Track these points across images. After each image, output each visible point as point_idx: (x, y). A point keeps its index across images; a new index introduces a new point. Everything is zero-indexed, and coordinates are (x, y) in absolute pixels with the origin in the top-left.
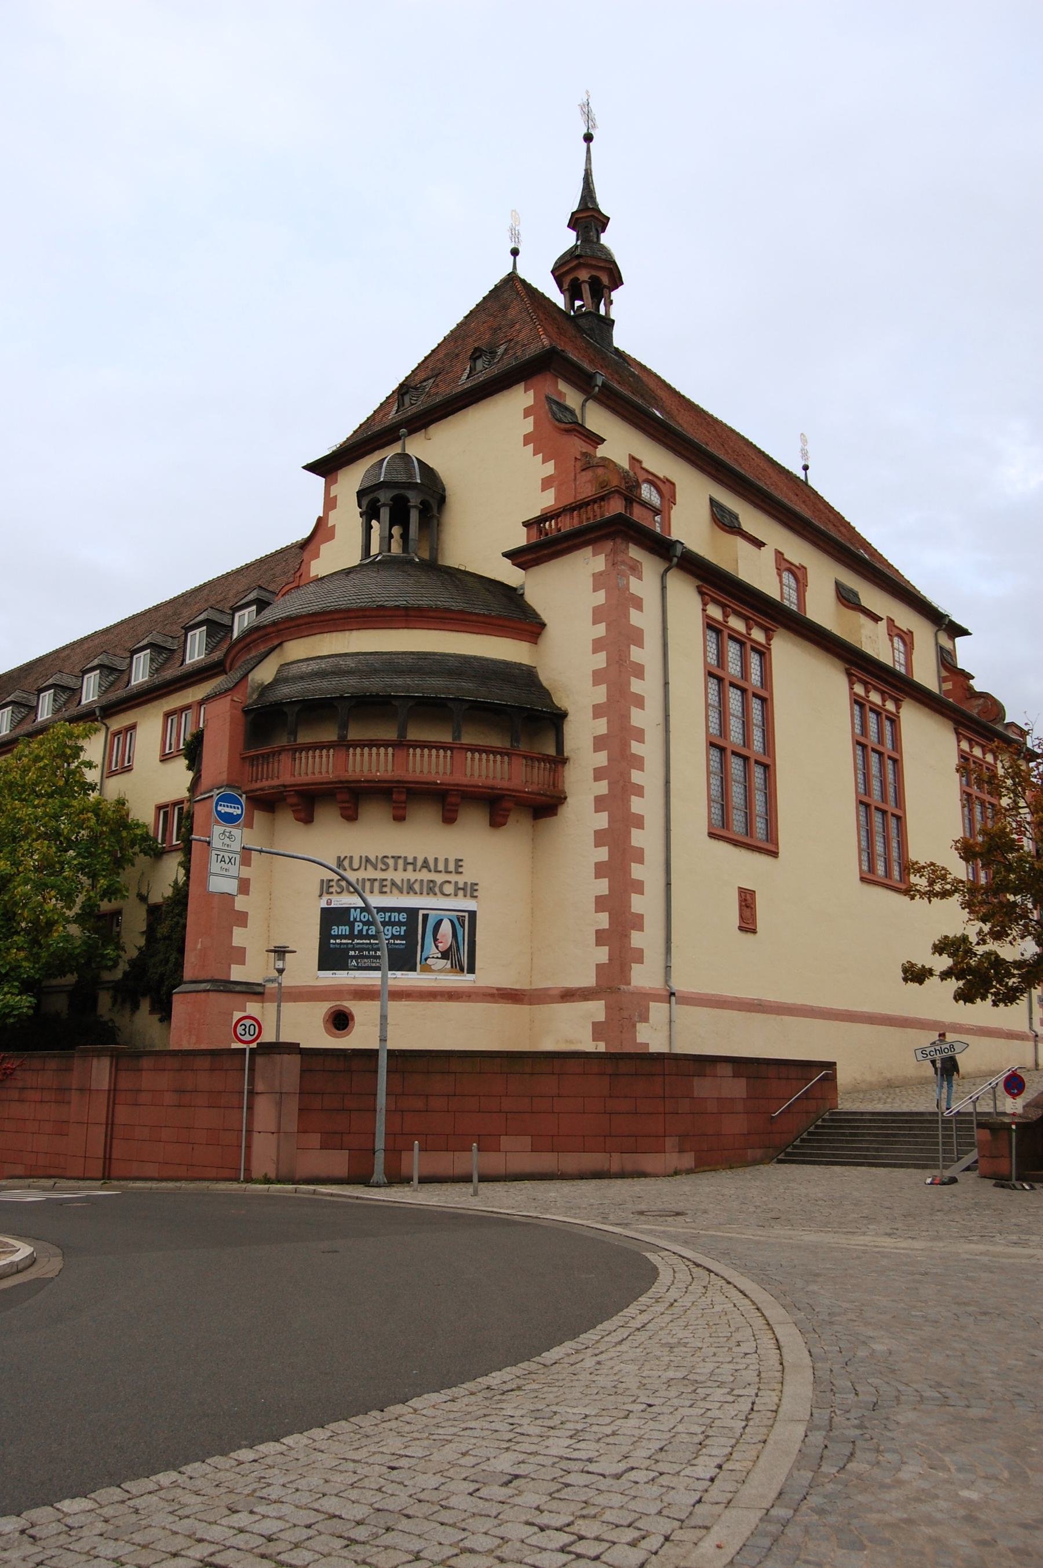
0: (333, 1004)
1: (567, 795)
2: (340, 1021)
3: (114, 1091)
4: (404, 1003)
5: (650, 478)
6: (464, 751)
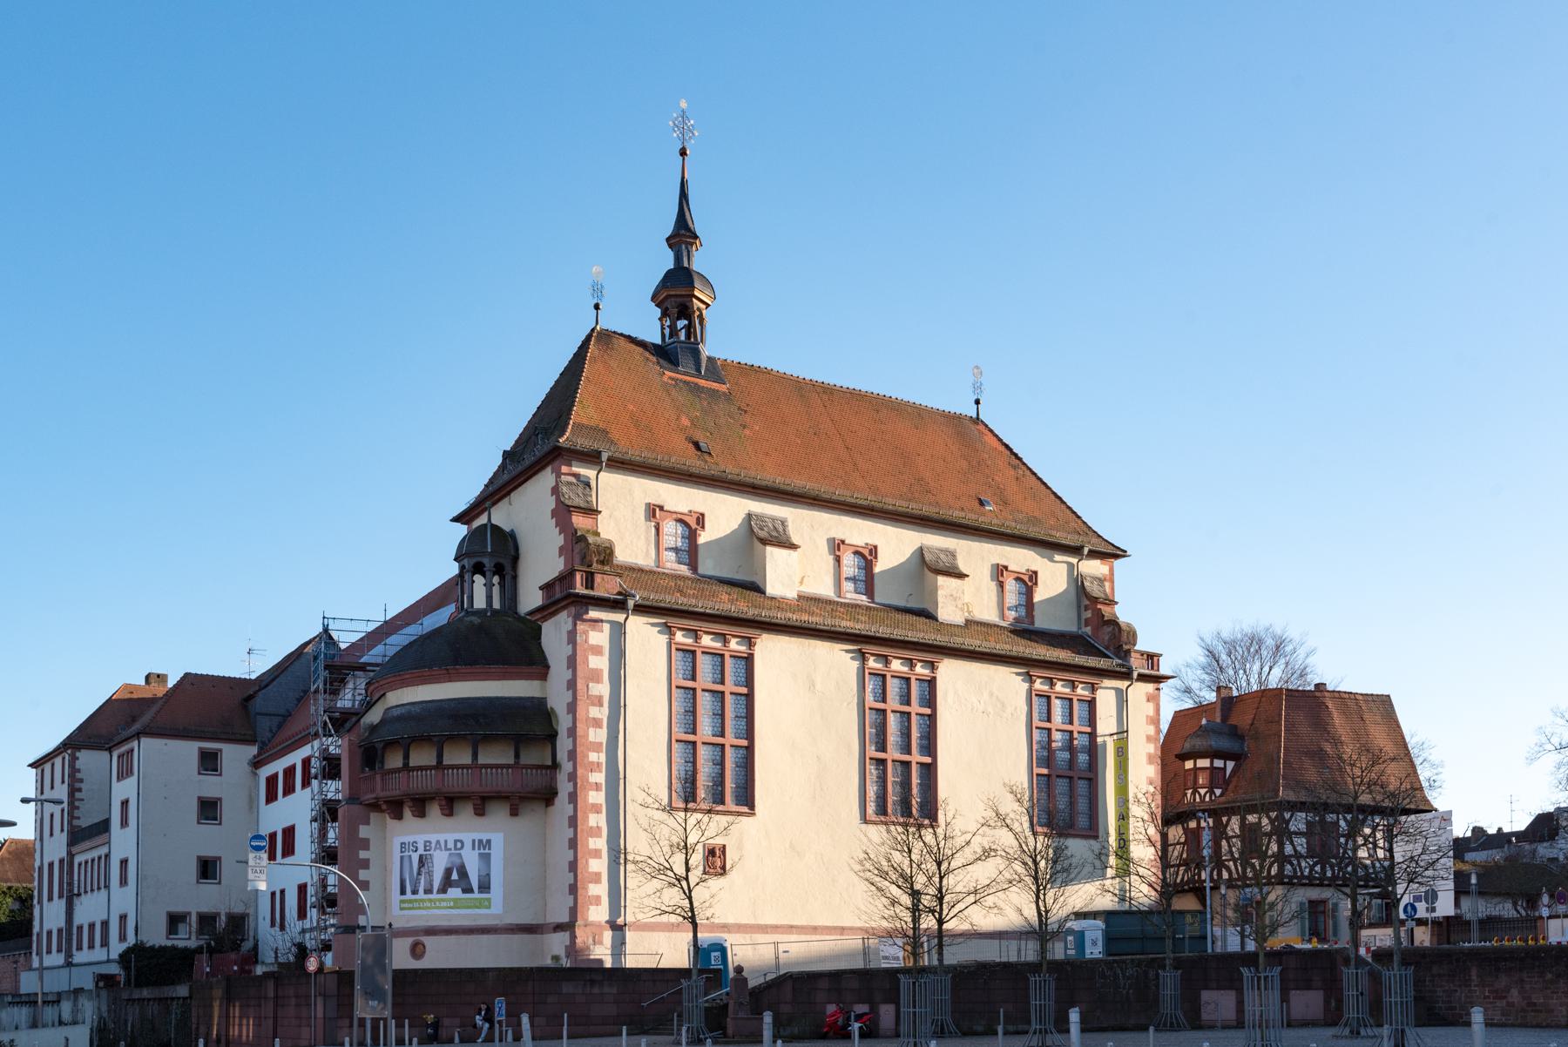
1: (559, 791)
2: (417, 951)
3: (276, 997)
6: (478, 769)
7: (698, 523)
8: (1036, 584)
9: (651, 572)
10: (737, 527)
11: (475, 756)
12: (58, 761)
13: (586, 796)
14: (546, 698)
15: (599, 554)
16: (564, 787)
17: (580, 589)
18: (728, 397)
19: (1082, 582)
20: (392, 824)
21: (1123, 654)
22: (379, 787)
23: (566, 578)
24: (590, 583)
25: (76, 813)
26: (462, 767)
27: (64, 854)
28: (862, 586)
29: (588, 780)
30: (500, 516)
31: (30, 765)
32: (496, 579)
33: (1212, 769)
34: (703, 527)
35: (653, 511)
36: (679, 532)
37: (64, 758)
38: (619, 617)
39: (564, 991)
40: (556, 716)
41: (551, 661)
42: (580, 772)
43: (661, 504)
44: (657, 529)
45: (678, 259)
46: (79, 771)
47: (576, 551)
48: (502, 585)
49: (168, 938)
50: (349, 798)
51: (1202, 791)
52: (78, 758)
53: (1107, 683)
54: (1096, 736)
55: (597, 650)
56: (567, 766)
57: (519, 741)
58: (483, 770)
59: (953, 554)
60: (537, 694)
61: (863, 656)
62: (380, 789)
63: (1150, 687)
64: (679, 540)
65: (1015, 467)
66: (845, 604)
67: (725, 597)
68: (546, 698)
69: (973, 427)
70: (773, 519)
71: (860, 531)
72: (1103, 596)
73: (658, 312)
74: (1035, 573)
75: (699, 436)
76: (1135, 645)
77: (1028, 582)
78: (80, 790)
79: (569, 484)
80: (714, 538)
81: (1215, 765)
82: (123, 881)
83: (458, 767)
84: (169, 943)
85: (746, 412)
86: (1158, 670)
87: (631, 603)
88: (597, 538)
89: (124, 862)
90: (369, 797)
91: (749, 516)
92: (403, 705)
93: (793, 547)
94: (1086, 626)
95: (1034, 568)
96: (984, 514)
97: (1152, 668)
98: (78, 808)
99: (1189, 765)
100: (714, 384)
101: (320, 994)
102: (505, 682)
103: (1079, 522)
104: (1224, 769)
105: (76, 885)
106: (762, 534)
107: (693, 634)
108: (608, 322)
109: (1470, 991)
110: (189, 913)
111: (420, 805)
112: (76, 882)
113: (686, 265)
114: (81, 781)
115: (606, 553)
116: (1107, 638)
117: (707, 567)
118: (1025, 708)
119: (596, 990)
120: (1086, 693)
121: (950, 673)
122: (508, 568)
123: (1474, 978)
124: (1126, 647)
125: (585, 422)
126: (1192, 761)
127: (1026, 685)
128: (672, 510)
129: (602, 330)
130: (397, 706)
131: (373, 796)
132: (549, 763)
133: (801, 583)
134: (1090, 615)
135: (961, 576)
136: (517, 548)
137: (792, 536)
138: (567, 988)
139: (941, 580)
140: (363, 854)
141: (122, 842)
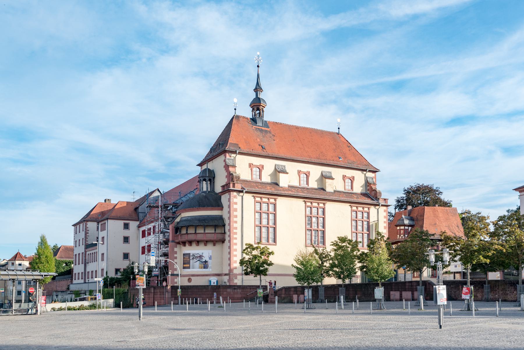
0: (189, 277)
2: (190, 280)
3: (154, 292)
4: (199, 277)
5: (256, 166)
9: (250, 181)
11: (205, 230)
12: (81, 225)
13: (233, 241)
14: (222, 215)
16: (227, 239)
17: (231, 188)
20: (183, 247)
21: (377, 199)
22: (180, 239)
23: (227, 185)
24: (234, 186)
25: (87, 240)
26: (201, 233)
27: (84, 251)
29: (233, 237)
30: (210, 166)
31: (73, 225)
32: (209, 182)
33: (405, 229)
37: (83, 224)
39: (228, 291)
40: (225, 220)
41: (224, 206)
42: (231, 235)
45: (257, 95)
46: (88, 228)
47: (230, 177)
48: (210, 184)
49: (115, 276)
50: (172, 241)
51: (402, 235)
52: (87, 224)
56: (228, 233)
57: (216, 227)
58: (207, 234)
59: (331, 173)
60: (220, 214)
61: (305, 202)
62: (180, 239)
63: (385, 208)
65: (349, 147)
67: (269, 188)
68: (222, 215)
69: (337, 136)
72: (373, 183)
73: (251, 109)
75: (262, 144)
76: (381, 196)
78: (88, 233)
81: (405, 228)
82: (103, 260)
83: (200, 233)
84: (116, 277)
86: (387, 203)
87: (244, 191)
88: (236, 174)
89: (103, 254)
90: (177, 241)
92: (186, 217)
93: (287, 173)
94: (368, 191)
96: (339, 161)
97: (386, 203)
98: (87, 238)
99: (398, 228)
101: (167, 292)
103: (367, 162)
104: (408, 229)
105: (87, 260)
106: (279, 170)
108: (237, 114)
109: (460, 292)
110: (121, 269)
111: (190, 243)
112: (87, 259)
113: (259, 97)
114: (88, 230)
115: (238, 178)
116: (373, 194)
119: (236, 291)
121: (329, 206)
122: (212, 180)
123: (460, 288)
124: (378, 197)
125: (232, 142)
126: (399, 227)
129: (237, 115)
130: (184, 217)
131: (178, 240)
132: (223, 232)
134: (369, 188)
135: (333, 179)
136: (214, 175)
137: (287, 170)
138: (229, 290)
139: (327, 180)
140: (175, 255)
141: (101, 249)
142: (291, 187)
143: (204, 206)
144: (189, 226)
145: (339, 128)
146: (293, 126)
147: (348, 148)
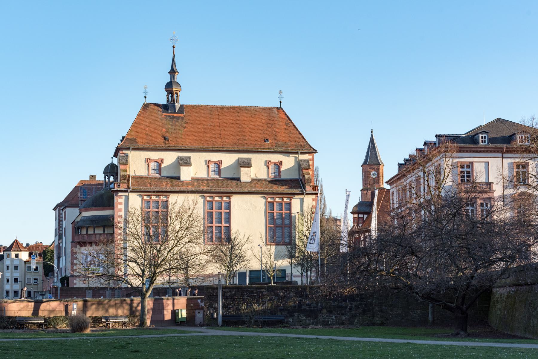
7: (161, 162)
8: (282, 165)
10: (174, 161)
15: (123, 178)
18: (183, 118)
19: (300, 163)
22: (80, 238)
24: (119, 186)
28: (217, 173)
31: (53, 210)
34: (163, 163)
35: (147, 160)
36: (156, 165)
38: (126, 194)
43: (149, 158)
44: (148, 165)
53: (296, 196)
54: (291, 214)
55: (121, 204)
59: (250, 159)
61: (205, 197)
64: (156, 167)
65: (286, 124)
66: (210, 179)
70: (186, 157)
71: (215, 157)
74: (282, 162)
77: (279, 165)
79: (122, 156)
80: (167, 165)
85: (187, 122)
87: (129, 191)
91: (178, 157)
95: (281, 160)
100: (180, 114)
102: (104, 211)
103: (304, 142)
107: (149, 196)
117: (164, 173)
118: (264, 207)
120: (288, 200)
127: (265, 200)
128: (153, 159)
133: (196, 174)
142: (195, 180)
143: (96, 206)
144: (89, 227)
145: (280, 102)
146: (217, 107)
147: (285, 126)
